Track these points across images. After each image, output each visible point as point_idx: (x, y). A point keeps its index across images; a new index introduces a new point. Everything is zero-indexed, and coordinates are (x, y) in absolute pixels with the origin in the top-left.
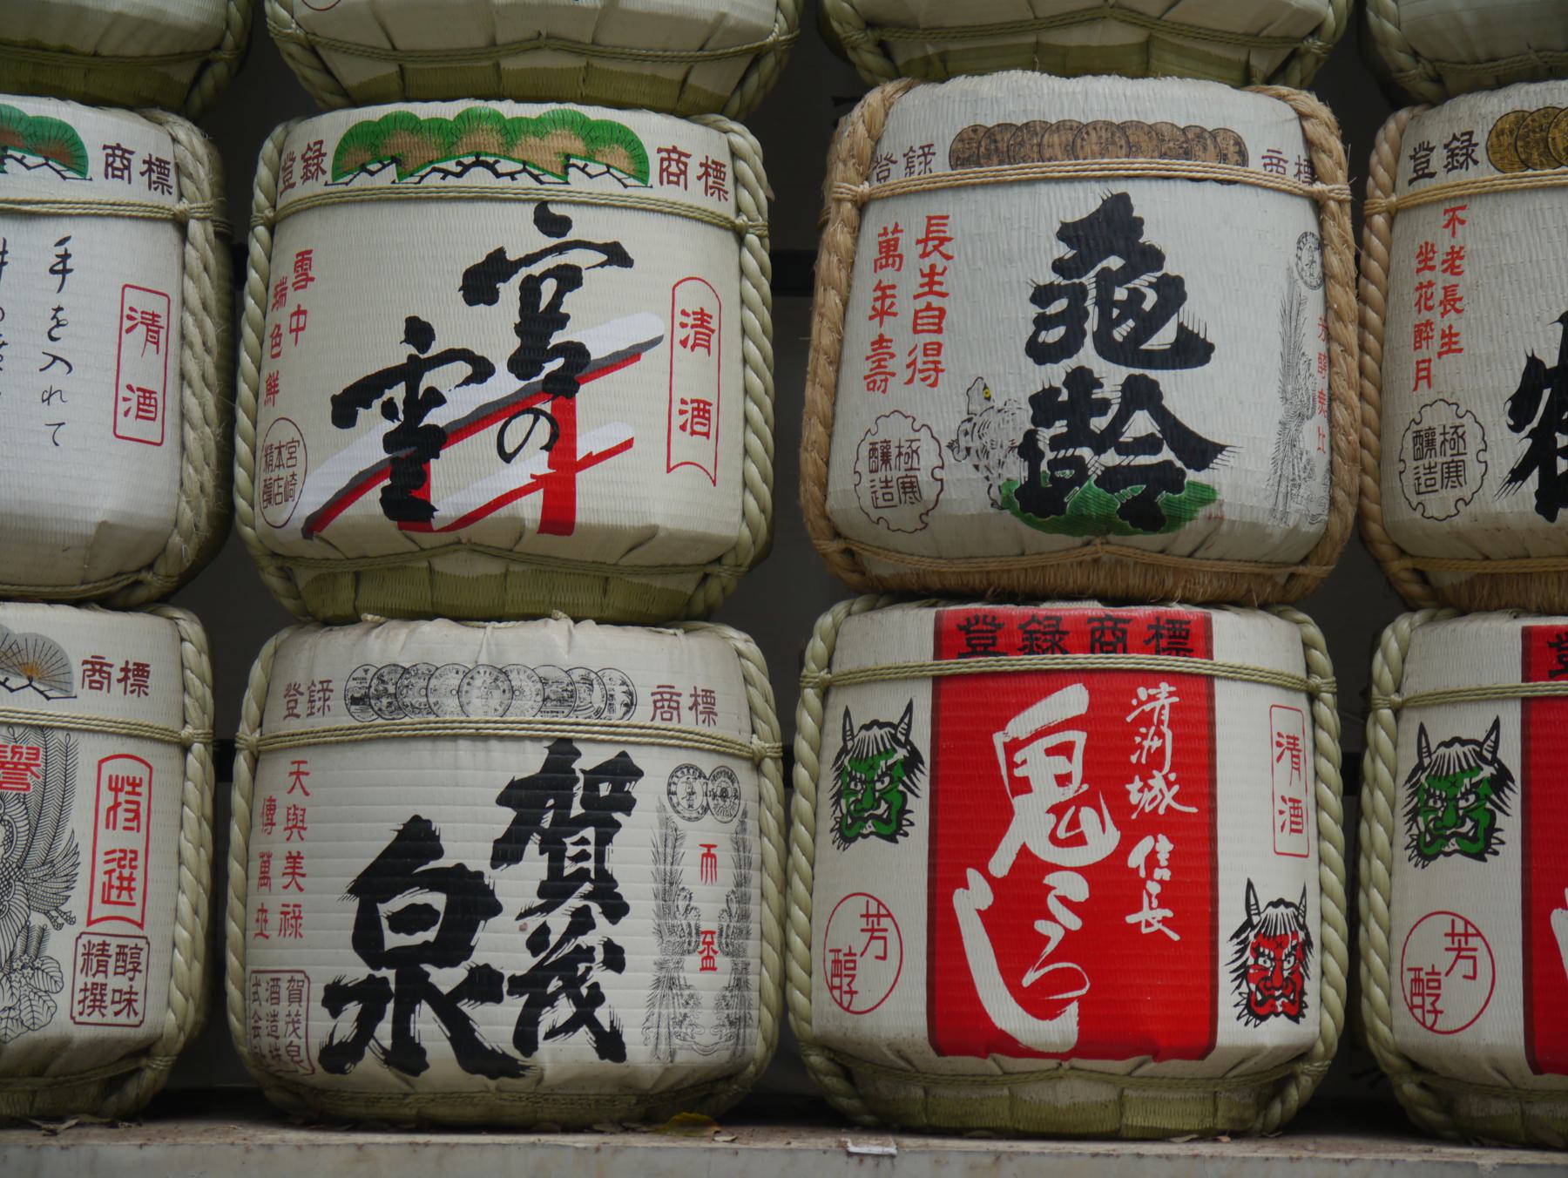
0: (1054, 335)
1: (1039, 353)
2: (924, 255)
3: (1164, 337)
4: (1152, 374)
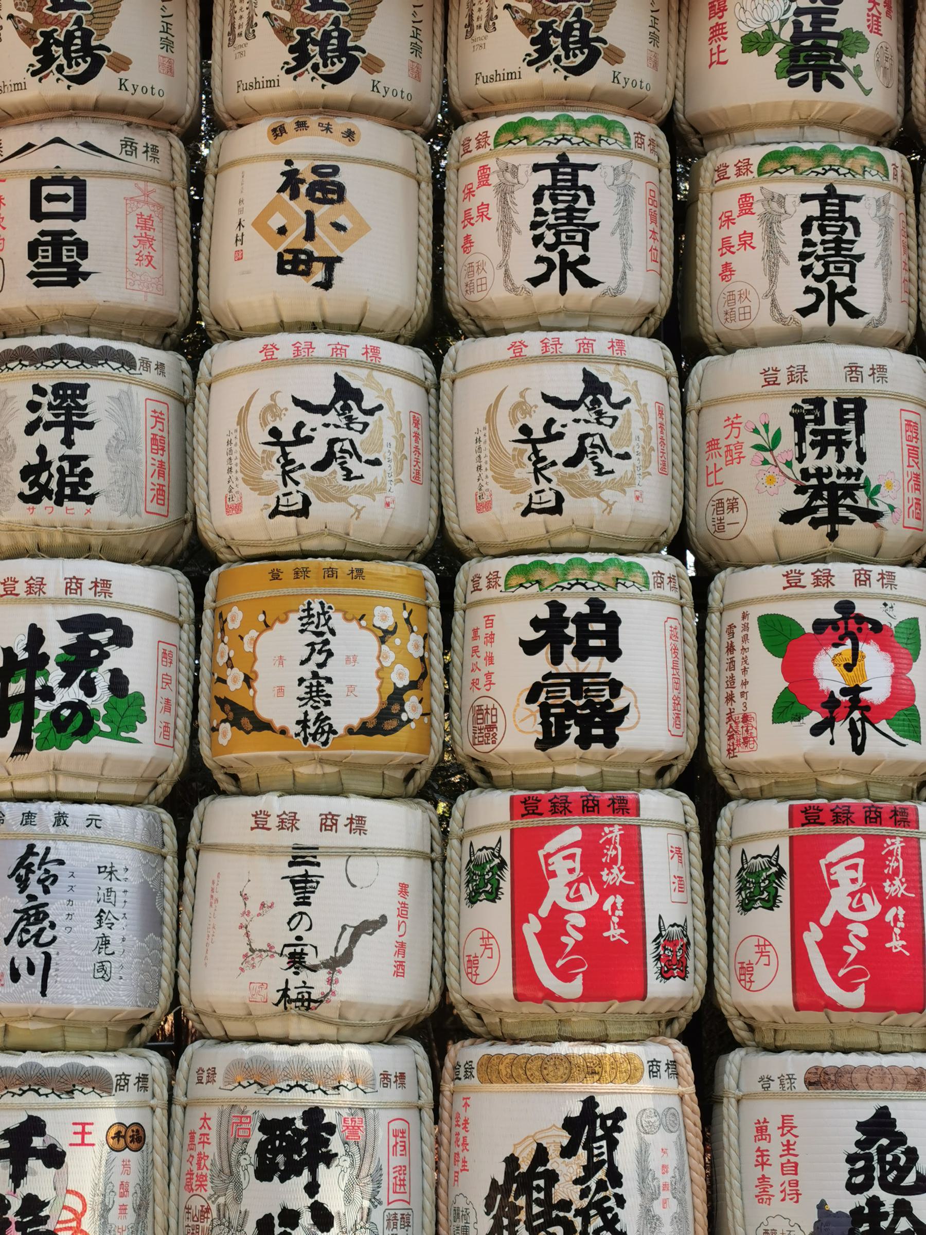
0: (859, 1179)
1: (853, 1189)
2: (783, 1135)
3: (910, 1179)
4: (907, 1198)
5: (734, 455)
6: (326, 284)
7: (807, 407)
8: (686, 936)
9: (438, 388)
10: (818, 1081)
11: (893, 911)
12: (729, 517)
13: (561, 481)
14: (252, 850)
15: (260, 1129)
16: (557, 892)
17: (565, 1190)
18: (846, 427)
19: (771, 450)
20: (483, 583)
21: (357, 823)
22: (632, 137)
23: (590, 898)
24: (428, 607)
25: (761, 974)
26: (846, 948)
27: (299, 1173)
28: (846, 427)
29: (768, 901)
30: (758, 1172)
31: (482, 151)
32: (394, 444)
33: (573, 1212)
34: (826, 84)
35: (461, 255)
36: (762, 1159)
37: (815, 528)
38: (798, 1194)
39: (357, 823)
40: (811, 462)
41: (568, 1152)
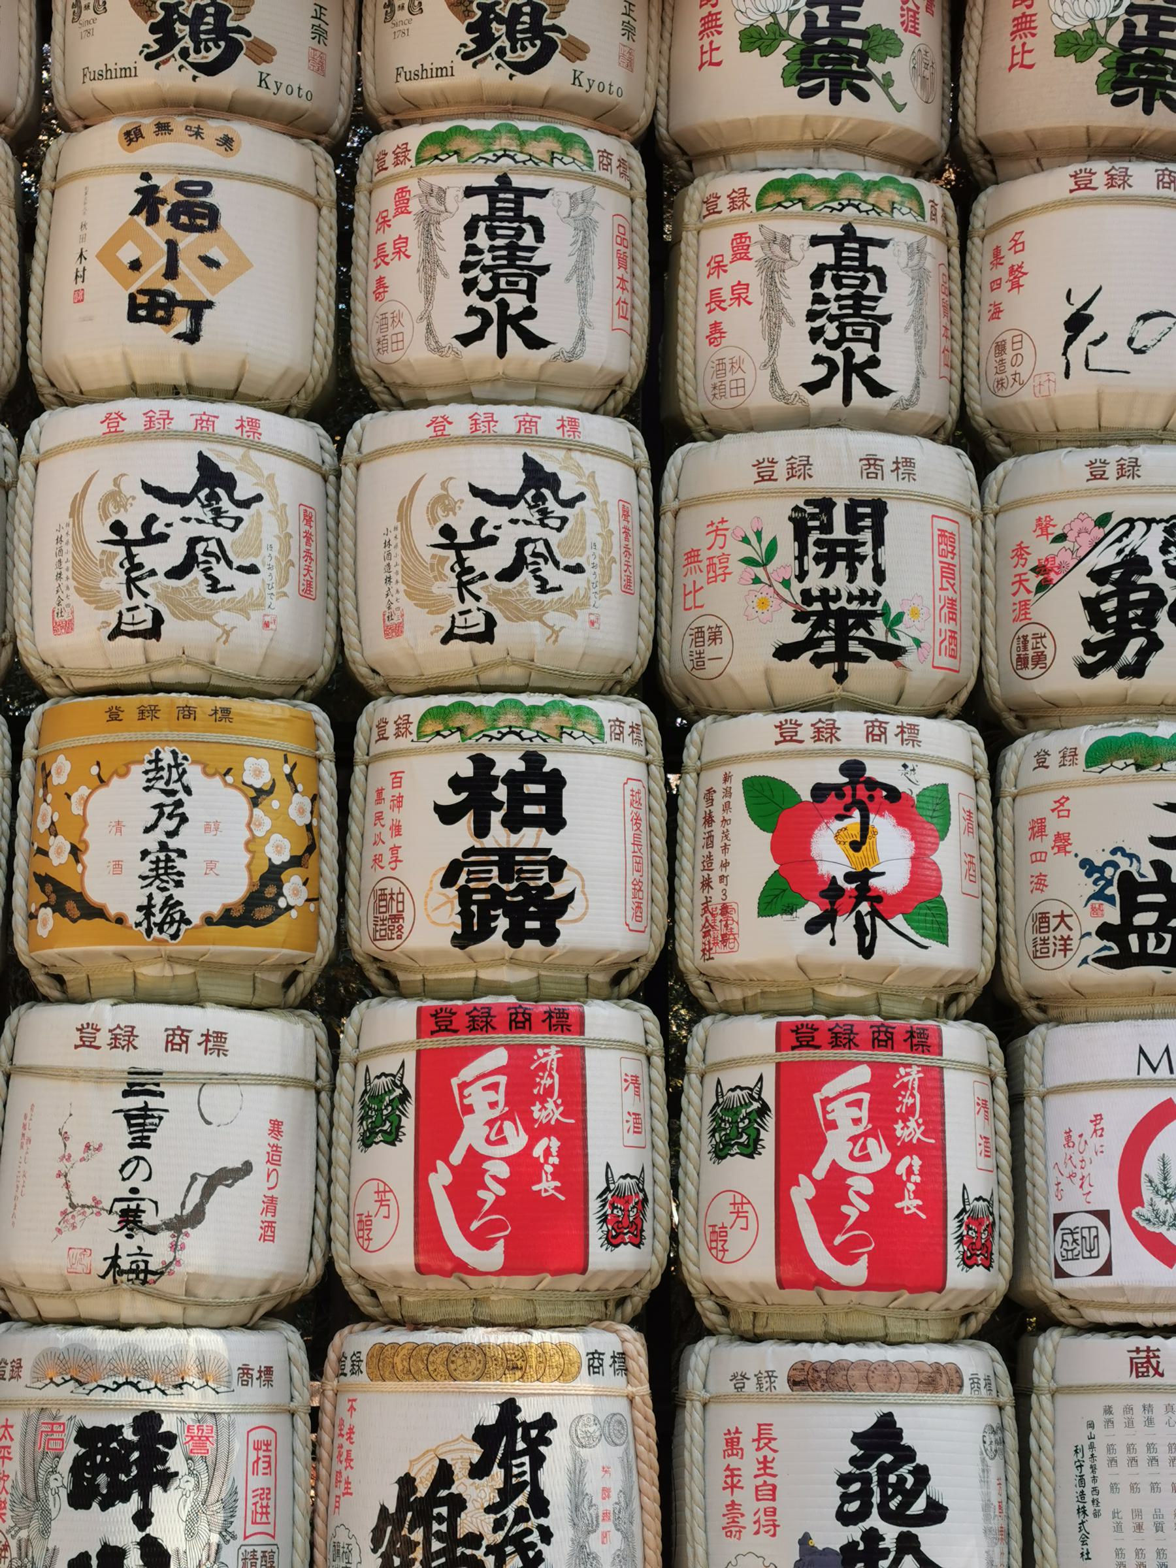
0: (853, 1507)
1: (845, 1518)
2: (758, 1449)
3: (919, 1506)
4: (914, 1530)
5: (717, 571)
6: (192, 337)
7: (810, 510)
8: (642, 1190)
9: (338, 474)
10: (805, 1379)
11: (906, 1161)
12: (710, 651)
13: (494, 599)
14: (75, 1075)
15: (76, 1440)
16: (473, 1134)
17: (475, 1520)
18: (860, 537)
19: (764, 565)
20: (391, 729)
21: (215, 1041)
22: (596, 156)
23: (516, 1140)
24: (319, 760)
25: (737, 1241)
26: (845, 1209)
27: (126, 1499)
28: (860, 537)
29: (747, 1146)
30: (727, 1498)
31: (401, 168)
32: (276, 547)
33: (483, 1549)
34: (846, 95)
35: (373, 304)
36: (732, 1480)
37: (818, 666)
38: (775, 1526)
39: (215, 1041)
40: (815, 581)
41: (479, 1471)
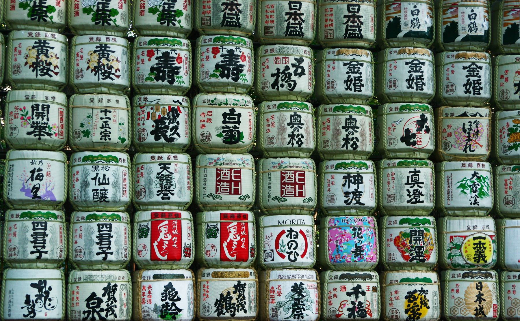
12: (14, 132)
40: (35, 120)
